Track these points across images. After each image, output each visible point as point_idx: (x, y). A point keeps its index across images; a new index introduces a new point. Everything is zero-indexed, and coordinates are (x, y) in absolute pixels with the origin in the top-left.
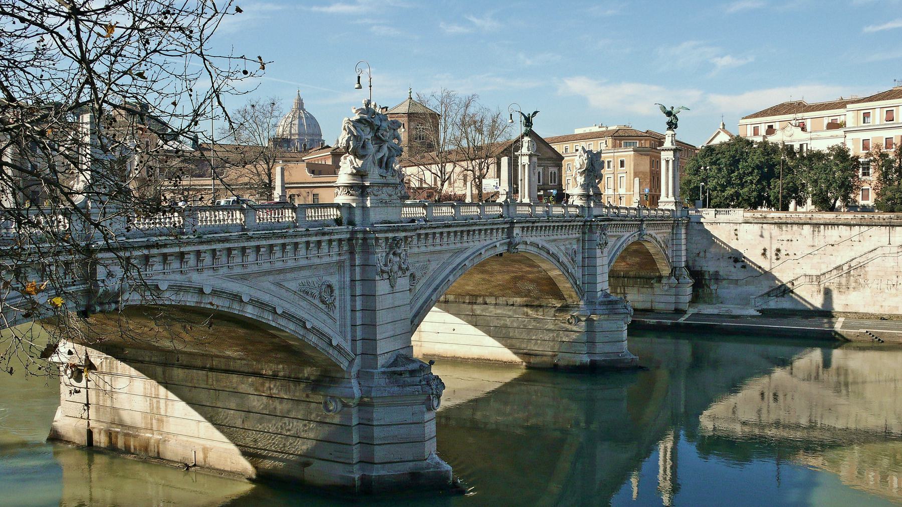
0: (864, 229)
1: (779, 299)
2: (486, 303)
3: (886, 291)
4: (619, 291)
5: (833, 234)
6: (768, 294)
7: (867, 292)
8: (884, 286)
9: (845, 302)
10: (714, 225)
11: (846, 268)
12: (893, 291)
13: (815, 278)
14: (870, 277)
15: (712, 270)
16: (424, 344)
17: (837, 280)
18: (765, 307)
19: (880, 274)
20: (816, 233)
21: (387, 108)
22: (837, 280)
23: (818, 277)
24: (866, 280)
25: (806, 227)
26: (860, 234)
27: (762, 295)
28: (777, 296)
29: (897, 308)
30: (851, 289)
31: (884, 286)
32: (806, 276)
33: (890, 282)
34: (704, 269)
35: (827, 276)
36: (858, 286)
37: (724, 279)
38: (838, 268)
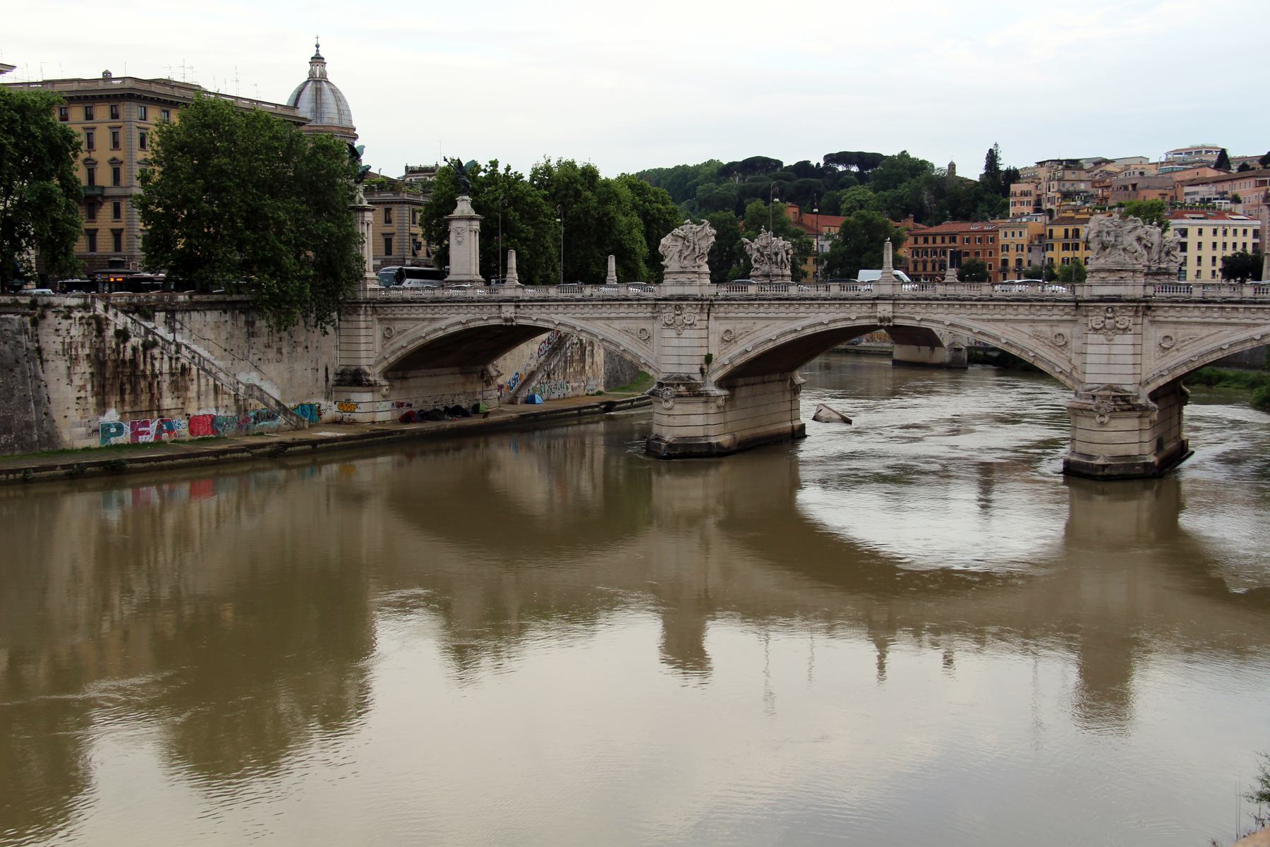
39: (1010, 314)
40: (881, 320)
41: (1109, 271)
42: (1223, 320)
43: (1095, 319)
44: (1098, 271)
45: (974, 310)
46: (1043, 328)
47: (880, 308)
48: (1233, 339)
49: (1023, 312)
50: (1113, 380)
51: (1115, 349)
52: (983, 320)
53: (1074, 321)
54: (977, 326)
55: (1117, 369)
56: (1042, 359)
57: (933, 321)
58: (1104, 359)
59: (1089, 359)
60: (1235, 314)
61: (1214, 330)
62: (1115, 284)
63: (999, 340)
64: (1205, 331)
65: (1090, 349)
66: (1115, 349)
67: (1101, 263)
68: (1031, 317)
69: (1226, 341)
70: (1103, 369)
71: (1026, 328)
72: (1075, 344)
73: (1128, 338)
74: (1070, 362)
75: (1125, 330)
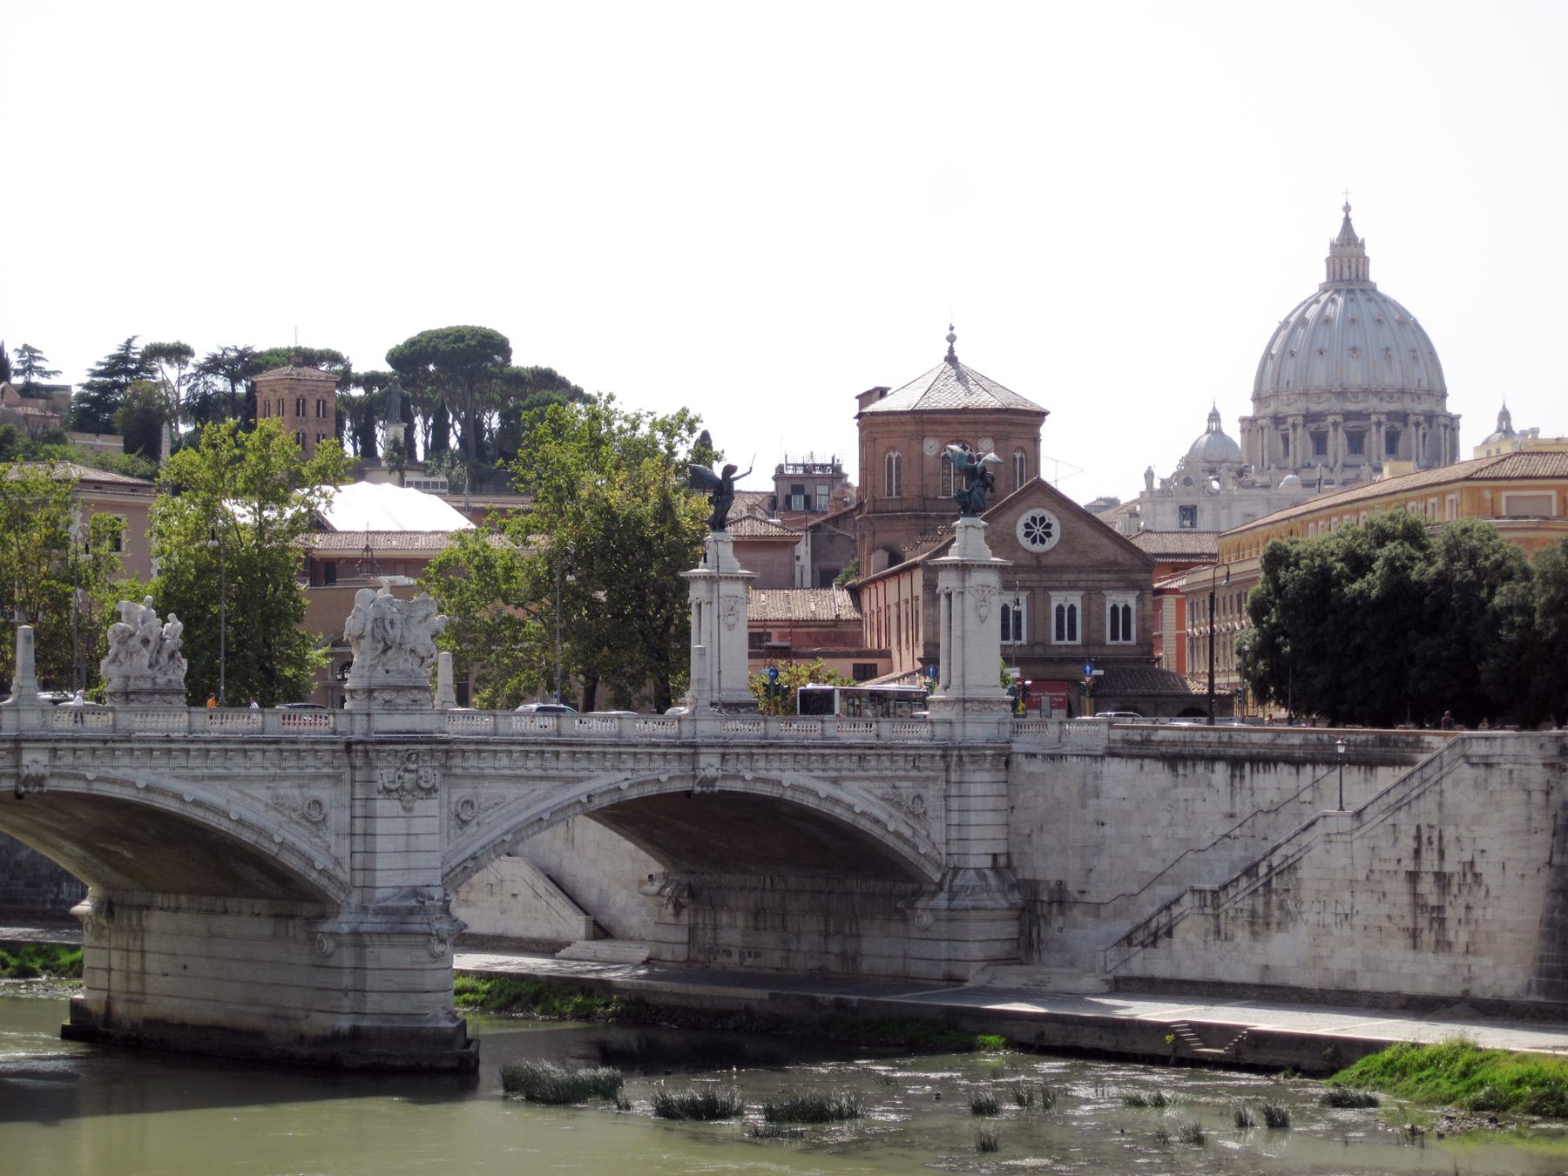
0: (1322, 771)
1: (1149, 950)
2: (226, 912)
3: (1336, 931)
4: (847, 931)
5: (1271, 784)
6: (1128, 939)
7: (1302, 929)
8: (1330, 919)
9: (1262, 961)
10: (1057, 762)
11: (1263, 870)
12: (1346, 931)
13: (1209, 896)
14: (1307, 895)
15: (1052, 877)
16: (149, 999)
17: (1249, 901)
18: (1122, 972)
19: (1325, 886)
20: (1237, 780)
21: (882, 393)
22: (1246, 904)
23: (1215, 893)
24: (1299, 902)
25: (1221, 770)
26: (1316, 782)
27: (1118, 944)
28: (1143, 945)
29: (1353, 973)
30: (1274, 926)
31: (1330, 919)
32: (1193, 891)
33: (1340, 910)
34: (1039, 876)
35: (1232, 892)
36: (1288, 917)
37: (1076, 902)
38: (1251, 871)
39: (238, 766)
40: (27, 781)
41: (399, 689)
42: (539, 772)
43: (385, 773)
44: (383, 688)
45: (182, 761)
46: (288, 790)
47: (27, 758)
48: (551, 802)
49: (258, 764)
50: (417, 879)
51: (418, 826)
52: (195, 779)
53: (336, 779)
54: (191, 791)
55: (421, 860)
56: (292, 849)
57: (114, 781)
58: (401, 842)
59: (382, 844)
60: (554, 764)
61: (524, 789)
62: (408, 712)
63: (226, 815)
64: (511, 791)
65: (381, 826)
66: (418, 826)
67: (380, 678)
68: (272, 771)
69: (542, 806)
70: (399, 862)
71: (261, 792)
72: (338, 818)
73: (430, 806)
74: (328, 849)
75: (431, 791)
